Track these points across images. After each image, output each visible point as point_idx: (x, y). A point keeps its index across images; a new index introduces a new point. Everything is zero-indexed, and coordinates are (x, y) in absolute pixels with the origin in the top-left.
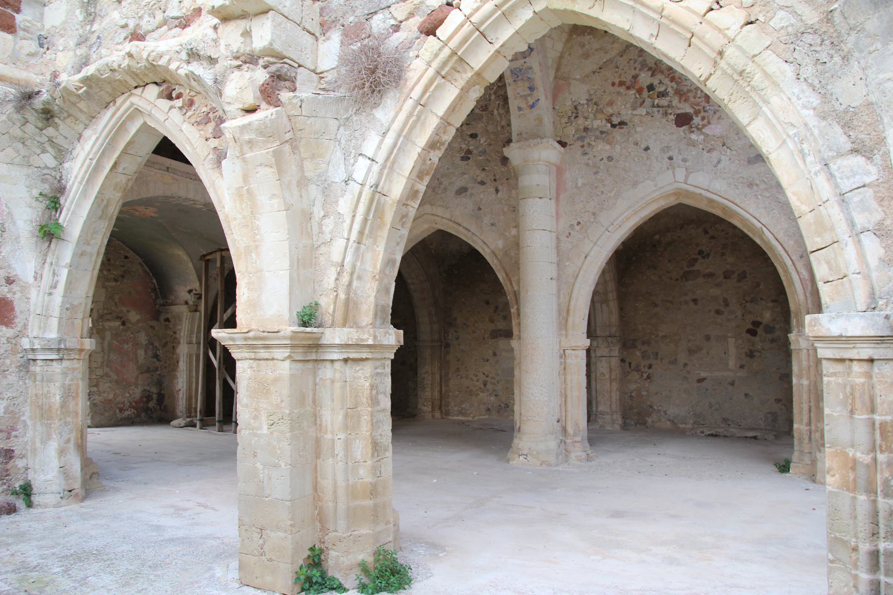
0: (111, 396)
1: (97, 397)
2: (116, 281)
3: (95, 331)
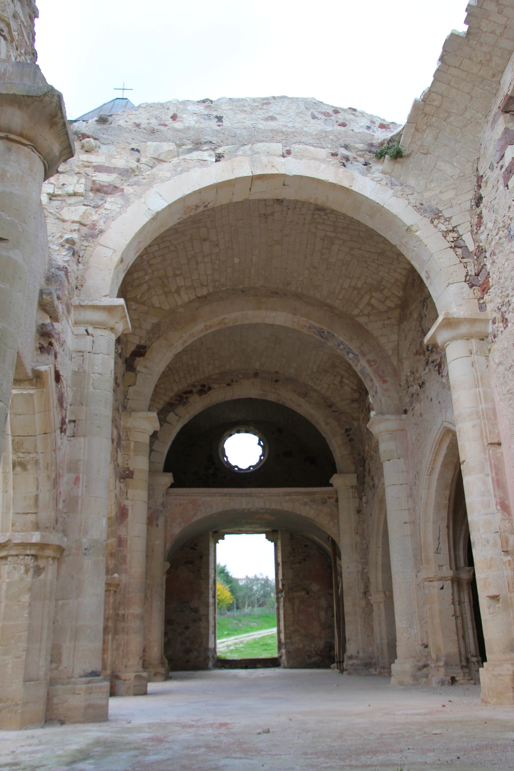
0: (301, 646)
2: (300, 563)
3: (287, 599)
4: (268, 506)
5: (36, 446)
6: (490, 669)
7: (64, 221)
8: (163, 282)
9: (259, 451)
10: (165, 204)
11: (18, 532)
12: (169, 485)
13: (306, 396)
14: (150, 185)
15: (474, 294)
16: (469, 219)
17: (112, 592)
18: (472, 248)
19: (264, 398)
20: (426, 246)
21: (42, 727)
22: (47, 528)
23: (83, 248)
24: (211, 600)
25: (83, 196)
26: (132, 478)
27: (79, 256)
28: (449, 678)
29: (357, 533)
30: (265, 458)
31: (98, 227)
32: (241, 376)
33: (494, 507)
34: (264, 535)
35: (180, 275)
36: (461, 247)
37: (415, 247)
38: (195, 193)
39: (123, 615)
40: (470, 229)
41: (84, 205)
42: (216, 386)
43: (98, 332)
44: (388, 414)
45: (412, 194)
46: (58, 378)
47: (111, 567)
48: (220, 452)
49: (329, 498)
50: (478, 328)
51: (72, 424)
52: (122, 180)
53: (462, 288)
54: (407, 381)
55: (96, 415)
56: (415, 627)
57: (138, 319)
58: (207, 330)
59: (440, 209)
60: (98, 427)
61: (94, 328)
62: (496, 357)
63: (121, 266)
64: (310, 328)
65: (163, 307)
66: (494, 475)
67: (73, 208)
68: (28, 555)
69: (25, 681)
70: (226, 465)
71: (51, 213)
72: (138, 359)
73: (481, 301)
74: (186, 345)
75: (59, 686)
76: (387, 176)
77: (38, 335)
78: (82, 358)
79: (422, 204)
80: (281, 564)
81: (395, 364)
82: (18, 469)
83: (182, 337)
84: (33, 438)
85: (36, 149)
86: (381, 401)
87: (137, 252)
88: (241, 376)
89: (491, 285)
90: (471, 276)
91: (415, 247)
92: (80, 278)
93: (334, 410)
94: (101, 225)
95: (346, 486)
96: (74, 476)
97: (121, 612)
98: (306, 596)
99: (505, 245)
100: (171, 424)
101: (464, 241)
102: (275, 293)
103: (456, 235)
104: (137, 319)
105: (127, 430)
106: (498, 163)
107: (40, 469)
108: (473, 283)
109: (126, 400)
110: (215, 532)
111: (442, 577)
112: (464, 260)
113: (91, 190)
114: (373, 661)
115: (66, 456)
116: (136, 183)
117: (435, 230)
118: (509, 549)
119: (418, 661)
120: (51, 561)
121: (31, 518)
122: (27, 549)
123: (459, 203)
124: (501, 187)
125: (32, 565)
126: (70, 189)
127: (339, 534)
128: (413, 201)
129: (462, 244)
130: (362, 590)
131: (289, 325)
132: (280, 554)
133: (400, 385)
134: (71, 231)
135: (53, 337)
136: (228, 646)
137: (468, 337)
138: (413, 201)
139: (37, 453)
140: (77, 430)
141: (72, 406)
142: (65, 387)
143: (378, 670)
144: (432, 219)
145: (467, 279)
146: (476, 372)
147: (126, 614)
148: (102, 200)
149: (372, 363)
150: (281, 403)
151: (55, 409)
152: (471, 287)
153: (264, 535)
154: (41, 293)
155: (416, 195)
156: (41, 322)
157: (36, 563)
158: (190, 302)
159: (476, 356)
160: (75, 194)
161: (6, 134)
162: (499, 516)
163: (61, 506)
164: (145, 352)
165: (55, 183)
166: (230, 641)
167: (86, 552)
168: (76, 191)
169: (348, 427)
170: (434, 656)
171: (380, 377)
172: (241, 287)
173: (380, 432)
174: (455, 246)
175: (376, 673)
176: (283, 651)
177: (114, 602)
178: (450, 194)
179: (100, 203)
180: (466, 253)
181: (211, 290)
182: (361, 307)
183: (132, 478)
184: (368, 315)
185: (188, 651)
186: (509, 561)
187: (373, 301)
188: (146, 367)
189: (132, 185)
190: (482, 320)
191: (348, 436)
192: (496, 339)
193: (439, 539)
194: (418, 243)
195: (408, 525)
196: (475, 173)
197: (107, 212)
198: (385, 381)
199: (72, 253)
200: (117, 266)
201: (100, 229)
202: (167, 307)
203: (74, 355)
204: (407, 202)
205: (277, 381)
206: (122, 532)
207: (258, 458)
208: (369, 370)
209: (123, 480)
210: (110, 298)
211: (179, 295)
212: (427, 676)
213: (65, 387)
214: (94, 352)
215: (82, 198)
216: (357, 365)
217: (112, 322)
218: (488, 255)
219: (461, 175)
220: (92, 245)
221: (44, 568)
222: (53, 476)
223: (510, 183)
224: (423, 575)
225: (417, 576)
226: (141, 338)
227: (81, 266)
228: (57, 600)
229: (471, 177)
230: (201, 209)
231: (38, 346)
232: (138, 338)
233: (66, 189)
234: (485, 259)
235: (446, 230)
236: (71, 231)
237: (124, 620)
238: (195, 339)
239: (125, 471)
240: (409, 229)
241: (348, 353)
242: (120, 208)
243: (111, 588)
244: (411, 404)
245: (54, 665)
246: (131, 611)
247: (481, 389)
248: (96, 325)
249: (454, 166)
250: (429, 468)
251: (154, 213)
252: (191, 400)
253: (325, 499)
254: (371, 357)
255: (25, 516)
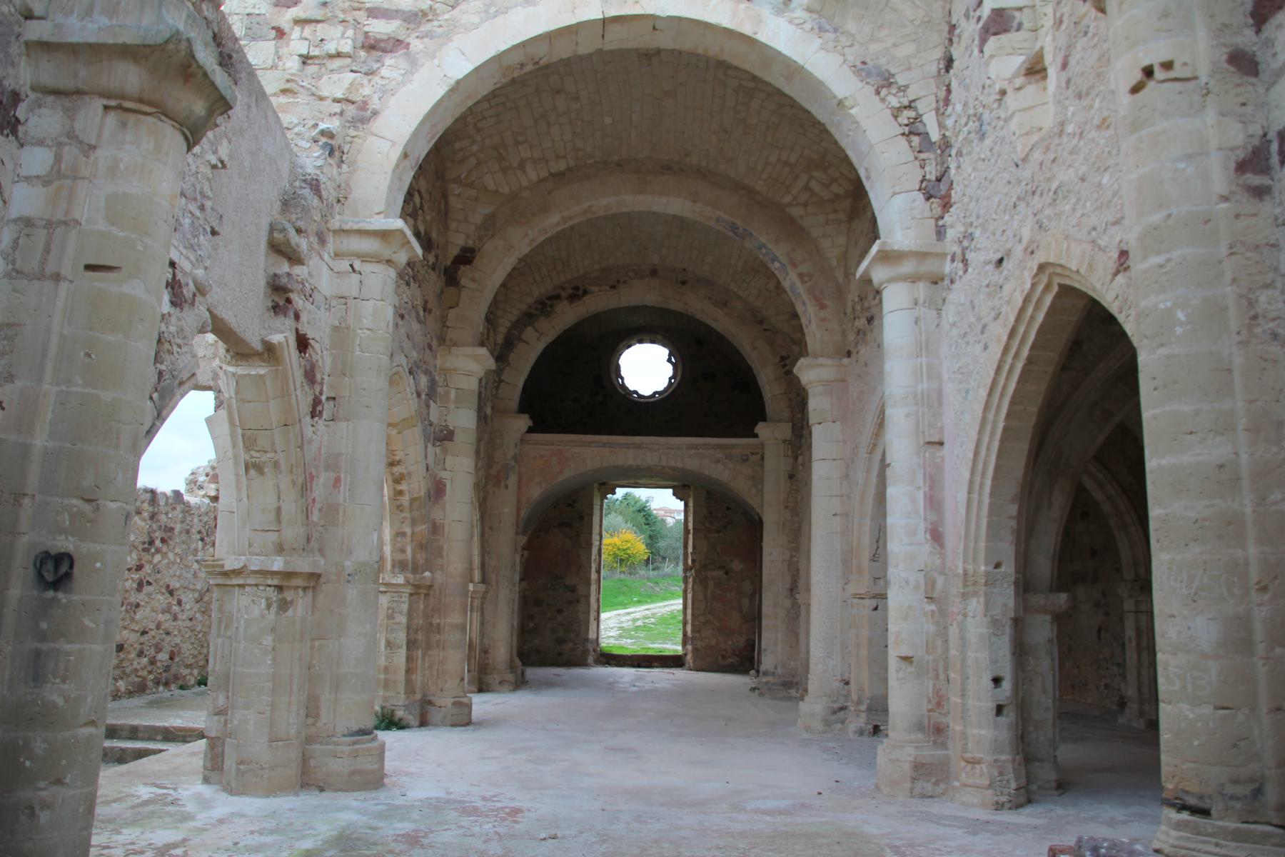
0: (713, 643)
1: (699, 642)
2: (718, 532)
3: (697, 580)
4: (664, 463)
5: (273, 443)
6: (887, 751)
7: (321, 99)
8: (500, 154)
9: (668, 370)
10: (470, 68)
11: (257, 555)
12: (526, 429)
13: (725, 306)
14: (448, 37)
15: (931, 210)
16: (934, 90)
17: (423, 595)
18: (935, 136)
19: (665, 306)
20: (865, 131)
21: (296, 794)
22: (294, 549)
23: (348, 139)
24: (594, 576)
25: (350, 57)
26: (452, 440)
27: (343, 153)
28: (870, 727)
29: (787, 507)
30: (677, 382)
31: (371, 107)
32: (631, 274)
33: (922, 536)
34: (670, 491)
35: (523, 143)
36: (919, 134)
37: (850, 130)
38: (515, 47)
39: (438, 625)
40: (934, 105)
41: (352, 71)
42: (594, 289)
43: (367, 268)
44: (822, 356)
45: (851, 46)
46: (303, 343)
47: (421, 563)
48: (613, 370)
49: (752, 453)
50: (929, 266)
51: (331, 403)
52: (408, 29)
53: (914, 201)
54: (854, 309)
55: (364, 389)
56: (834, 657)
57: (463, 209)
58: (565, 222)
59: (893, 71)
60: (367, 407)
61: (362, 261)
62: (950, 314)
63: (406, 163)
64: (718, 220)
65: (500, 190)
66: (927, 489)
67: (335, 77)
68: (270, 586)
69: (271, 741)
70: (620, 390)
71: (303, 87)
72: (463, 268)
73: (941, 223)
74: (535, 245)
75: (317, 746)
76: (815, 16)
77: (269, 291)
78: (344, 307)
79: (864, 63)
80: (692, 531)
81: (840, 280)
82: (252, 472)
83: (527, 234)
84: (269, 432)
85: (166, 115)
86: (815, 335)
87: (432, 138)
88: (631, 274)
89: (953, 201)
90: (929, 181)
91: (850, 130)
92: (343, 186)
93: (766, 327)
94: (375, 103)
95: (777, 439)
96: (333, 475)
97: (435, 621)
98: (725, 576)
99: (974, 145)
100: (528, 344)
101: (925, 125)
102: (666, 168)
103: (912, 114)
104: (462, 209)
105: (446, 371)
106: (975, 11)
107: (281, 473)
108: (932, 192)
109: (445, 329)
110: (603, 484)
111: (877, 594)
112: (922, 156)
113: (363, 47)
114: (795, 680)
115: (323, 448)
116: (428, 35)
117: (882, 106)
118: (935, 596)
119: (833, 702)
120: (301, 592)
121: (273, 537)
122: (268, 578)
123: (920, 63)
124: (976, 52)
125: (275, 599)
126: (331, 47)
127: (762, 505)
128: (851, 58)
129: (921, 129)
130: (788, 586)
131: (687, 214)
132: (691, 519)
133: (845, 313)
134: (330, 115)
135: (291, 291)
136: (635, 620)
137: (914, 279)
138: (851, 58)
139: (275, 452)
140: (338, 412)
141: (331, 378)
142: (319, 352)
143: (800, 691)
144: (878, 88)
145: (924, 185)
146: (920, 333)
147: (442, 624)
148: (378, 61)
149: (806, 279)
150: (690, 314)
151: (299, 392)
152: (928, 199)
153: (670, 491)
154: (272, 228)
155: (856, 47)
156: (272, 270)
157: (280, 596)
158: (541, 181)
159: (922, 309)
160: (339, 55)
161: (118, 102)
162: (927, 548)
163: (315, 517)
164: (474, 257)
165: (310, 37)
166: (640, 611)
167: (350, 578)
168: (340, 50)
169: (784, 354)
170: (854, 696)
171: (816, 299)
172: (616, 158)
173: (811, 382)
174: (911, 133)
175: (798, 695)
176: (689, 647)
177: (425, 608)
178: (907, 49)
179: (375, 66)
180: (927, 144)
181: (572, 163)
182: (794, 192)
183: (452, 440)
184: (805, 205)
185: (561, 641)
186: (933, 611)
187: (813, 184)
188: (473, 280)
189: (422, 38)
190: (936, 255)
191: (784, 366)
192: (954, 286)
193: (877, 542)
194: (855, 126)
195: (838, 518)
196: (947, 19)
197: (384, 83)
198: (823, 307)
199: (328, 152)
200: (397, 166)
201: (373, 109)
202: (505, 190)
203: (334, 303)
204: (841, 58)
205: (684, 283)
206: (437, 514)
207: (668, 380)
208: (800, 288)
209: (439, 443)
210: (385, 218)
211: (524, 172)
212: (843, 722)
213: (319, 352)
214: (361, 297)
215: (349, 60)
216: (785, 279)
217: (387, 253)
218: (953, 152)
219: (926, 19)
220: (361, 134)
221: (291, 602)
222: (300, 480)
223: (986, 49)
224: (851, 589)
225: (844, 589)
226: (468, 236)
227: (344, 167)
228: (312, 640)
229: (940, 24)
230: (530, 67)
231: (270, 304)
232: (463, 236)
233: (326, 47)
234: (950, 158)
235: (899, 105)
236: (330, 115)
237: (439, 632)
238: (549, 235)
239: (442, 431)
240: (840, 103)
241: (773, 261)
242: (403, 75)
243: (421, 591)
244: (856, 345)
245: (311, 720)
246: (449, 620)
247: (924, 360)
248: (366, 258)
249: (914, 4)
250: (869, 444)
251: (452, 82)
252: (558, 309)
253: (747, 455)
254: (804, 268)
255: (264, 534)
